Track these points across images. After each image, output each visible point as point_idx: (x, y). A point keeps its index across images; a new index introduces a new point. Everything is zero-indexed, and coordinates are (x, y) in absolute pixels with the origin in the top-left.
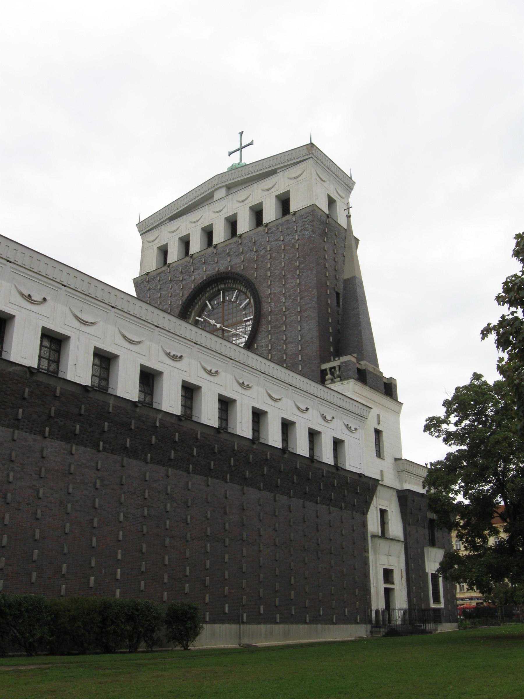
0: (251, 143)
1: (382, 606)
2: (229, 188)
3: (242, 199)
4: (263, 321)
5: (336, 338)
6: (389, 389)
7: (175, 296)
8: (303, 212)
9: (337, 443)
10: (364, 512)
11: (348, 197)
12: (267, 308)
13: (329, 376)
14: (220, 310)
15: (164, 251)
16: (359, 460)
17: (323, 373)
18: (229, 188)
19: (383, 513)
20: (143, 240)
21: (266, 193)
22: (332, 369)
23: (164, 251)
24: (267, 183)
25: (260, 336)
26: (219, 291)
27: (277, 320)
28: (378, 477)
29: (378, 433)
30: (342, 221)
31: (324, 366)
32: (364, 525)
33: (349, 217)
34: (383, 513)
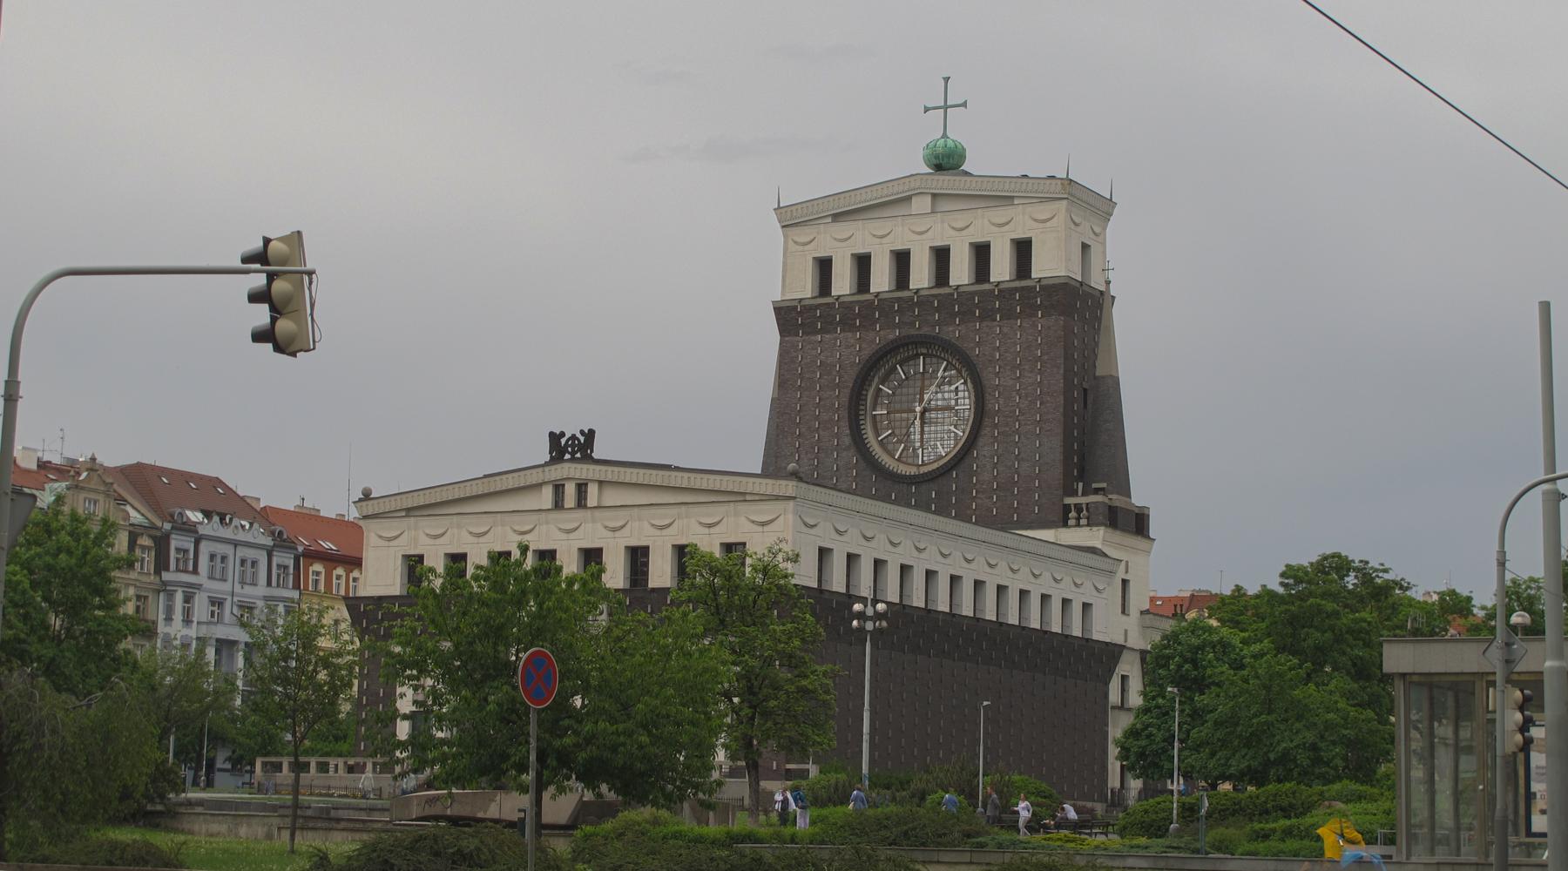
0: (964, 105)
1: (1117, 785)
2: (934, 196)
3: (960, 225)
4: (987, 421)
5: (1084, 465)
6: (1138, 524)
7: (848, 347)
8: (1051, 282)
9: (1086, 607)
10: (1107, 684)
11: (1104, 229)
12: (993, 405)
13: (1073, 514)
14: (919, 383)
15: (824, 266)
16: (1108, 627)
17: (1067, 509)
18: (934, 196)
19: (1124, 678)
20: (785, 236)
21: (996, 229)
22: (1078, 508)
23: (824, 266)
24: (1001, 214)
25: (981, 441)
26: (917, 356)
27: (1007, 425)
28: (1120, 641)
29: (1125, 582)
30: (1097, 282)
31: (1069, 500)
32: (1106, 696)
33: (1108, 283)
34: (1124, 678)
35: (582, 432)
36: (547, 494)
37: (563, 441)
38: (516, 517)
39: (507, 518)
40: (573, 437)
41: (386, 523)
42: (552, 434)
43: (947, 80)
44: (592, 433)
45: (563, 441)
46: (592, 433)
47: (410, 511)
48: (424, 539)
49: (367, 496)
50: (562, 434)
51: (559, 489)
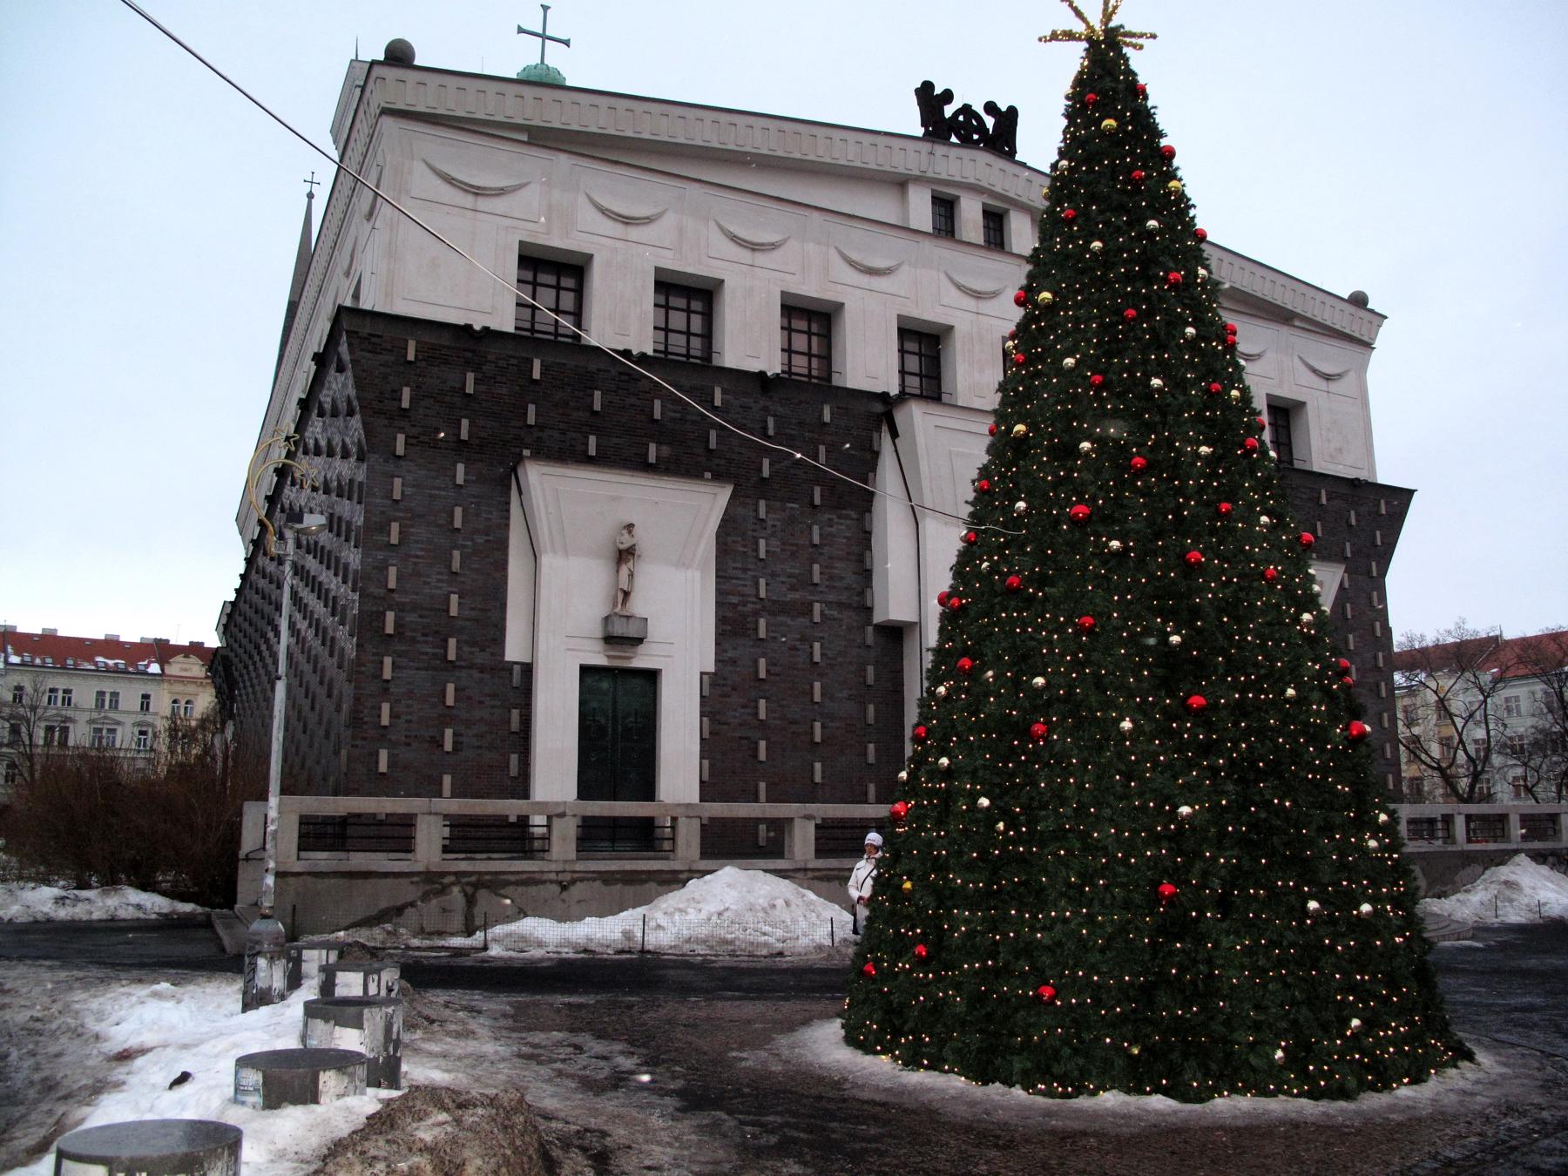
35: (991, 108)
36: (920, 210)
37: (949, 111)
38: (858, 232)
39: (838, 228)
40: (966, 109)
41: (476, 147)
42: (927, 87)
43: (545, 8)
44: (1013, 111)
45: (949, 111)
46: (1013, 111)
47: (542, 138)
48: (589, 218)
49: (399, 55)
50: (948, 96)
51: (945, 207)
